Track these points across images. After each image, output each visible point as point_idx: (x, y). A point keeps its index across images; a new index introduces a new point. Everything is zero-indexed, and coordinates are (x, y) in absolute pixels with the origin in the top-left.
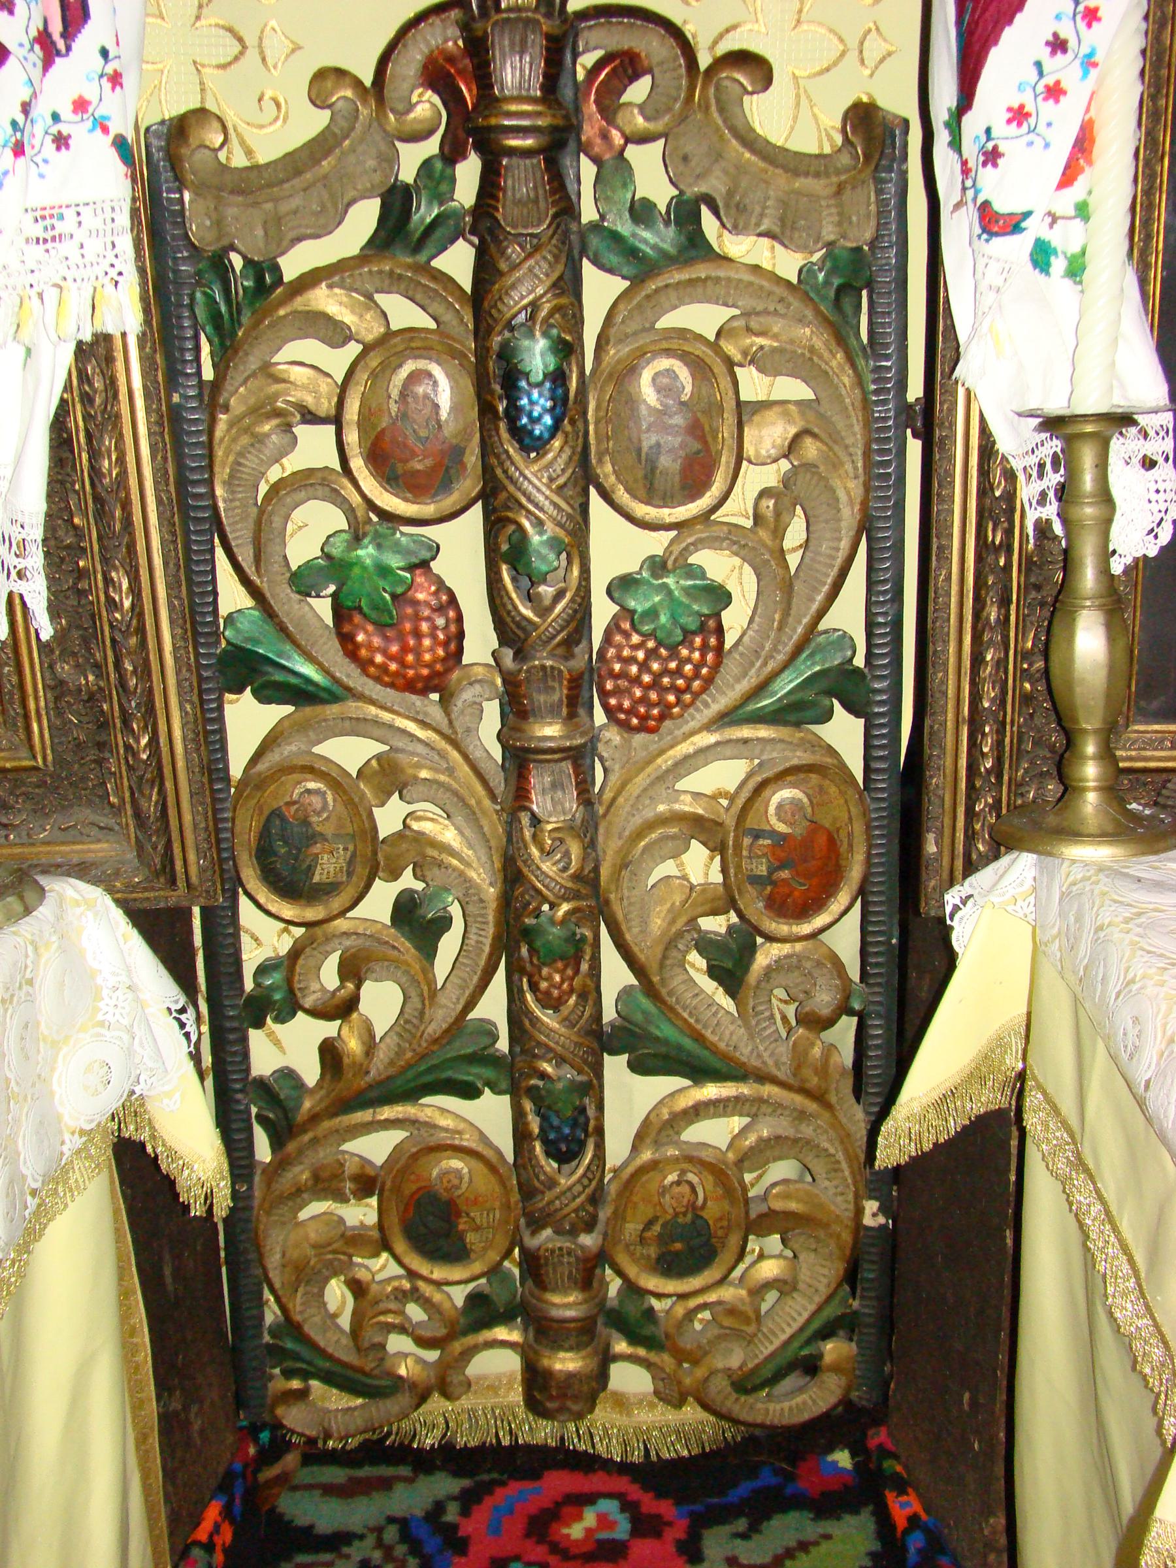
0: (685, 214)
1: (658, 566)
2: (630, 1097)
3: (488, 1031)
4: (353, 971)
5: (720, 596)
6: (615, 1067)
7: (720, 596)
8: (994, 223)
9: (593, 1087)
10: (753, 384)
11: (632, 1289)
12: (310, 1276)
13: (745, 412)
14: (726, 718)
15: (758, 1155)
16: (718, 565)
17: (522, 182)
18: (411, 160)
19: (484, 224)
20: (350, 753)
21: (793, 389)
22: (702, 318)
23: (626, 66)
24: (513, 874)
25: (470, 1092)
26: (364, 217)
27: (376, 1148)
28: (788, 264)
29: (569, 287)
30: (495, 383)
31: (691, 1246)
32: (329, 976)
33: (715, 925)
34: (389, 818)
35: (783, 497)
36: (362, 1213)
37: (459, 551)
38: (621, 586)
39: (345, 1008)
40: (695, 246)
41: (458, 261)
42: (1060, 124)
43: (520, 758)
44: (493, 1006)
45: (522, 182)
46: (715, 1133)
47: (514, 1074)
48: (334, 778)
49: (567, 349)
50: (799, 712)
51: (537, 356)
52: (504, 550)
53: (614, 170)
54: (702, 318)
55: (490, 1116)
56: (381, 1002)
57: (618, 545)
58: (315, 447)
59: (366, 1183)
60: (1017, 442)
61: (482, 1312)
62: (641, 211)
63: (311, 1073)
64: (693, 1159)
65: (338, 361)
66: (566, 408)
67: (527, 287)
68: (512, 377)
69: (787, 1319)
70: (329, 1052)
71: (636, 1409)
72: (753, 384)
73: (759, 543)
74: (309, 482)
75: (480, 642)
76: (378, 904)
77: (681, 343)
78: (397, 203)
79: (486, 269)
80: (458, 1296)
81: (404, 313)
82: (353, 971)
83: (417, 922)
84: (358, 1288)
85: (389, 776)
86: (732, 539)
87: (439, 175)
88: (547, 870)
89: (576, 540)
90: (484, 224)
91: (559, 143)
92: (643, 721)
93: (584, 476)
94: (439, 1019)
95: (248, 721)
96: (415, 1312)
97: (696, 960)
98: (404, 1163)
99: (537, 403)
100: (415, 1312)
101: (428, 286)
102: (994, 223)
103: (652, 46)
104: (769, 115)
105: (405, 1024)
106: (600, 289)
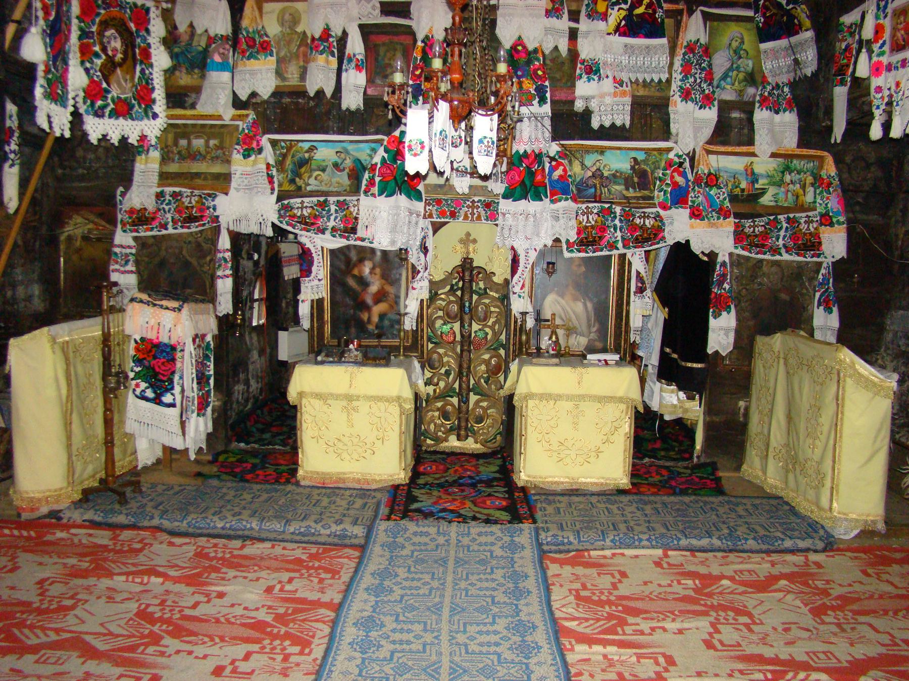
0: (485, 289)
1: (480, 330)
2: (473, 398)
3: (455, 389)
4: (439, 380)
5: (487, 334)
6: (471, 393)
7: (487, 334)
8: (514, 293)
9: (468, 394)
10: (492, 309)
11: (472, 426)
12: (429, 424)
13: (491, 312)
14: (488, 349)
15: (489, 408)
16: (487, 330)
17: (467, 285)
18: (454, 282)
19: (462, 289)
20: (441, 351)
21: (497, 310)
22: (487, 301)
23: (479, 273)
24: (460, 367)
25: (452, 397)
26: (448, 288)
27: (439, 404)
28: (496, 295)
29: (471, 297)
30: (462, 307)
31: (479, 420)
32: (436, 380)
33: (485, 375)
34: (445, 359)
35: (494, 323)
36: (437, 414)
37: (457, 326)
38: (476, 332)
39: (437, 384)
40: (486, 293)
41: (459, 293)
42: (520, 284)
43: (462, 351)
44: (456, 385)
45: (467, 285)
46: (485, 404)
47: (459, 395)
48: (438, 353)
49: (471, 303)
50: (496, 349)
51: (467, 304)
52: (462, 326)
53: (477, 284)
54: (487, 301)
55: (455, 400)
56: (442, 384)
57: (475, 327)
58: (440, 313)
59: (438, 409)
60: (518, 316)
61: (451, 429)
62: (480, 289)
63: (432, 393)
64: (482, 407)
65: (444, 303)
66: (470, 310)
67: (466, 297)
68: (464, 306)
69: (493, 431)
70: (435, 391)
71: (471, 445)
72: (492, 309)
73: (492, 328)
74: (439, 317)
75: (458, 338)
76: (443, 371)
77: (484, 304)
78: (452, 286)
79: (462, 294)
80: (448, 427)
81: (452, 298)
82: (439, 380)
83: (447, 373)
84: (435, 425)
85: (446, 354)
86: (489, 327)
87: (457, 283)
88: (465, 366)
89: (470, 326)
90: (462, 289)
91: (471, 281)
92: (477, 348)
93: (471, 319)
94: (449, 386)
95: (431, 346)
96: (442, 429)
97: (482, 381)
98: (443, 406)
99: (467, 309)
100: (442, 429)
101: (455, 295)
102: (514, 293)
103: (482, 271)
104: (495, 279)
105: (445, 388)
106: (475, 297)
